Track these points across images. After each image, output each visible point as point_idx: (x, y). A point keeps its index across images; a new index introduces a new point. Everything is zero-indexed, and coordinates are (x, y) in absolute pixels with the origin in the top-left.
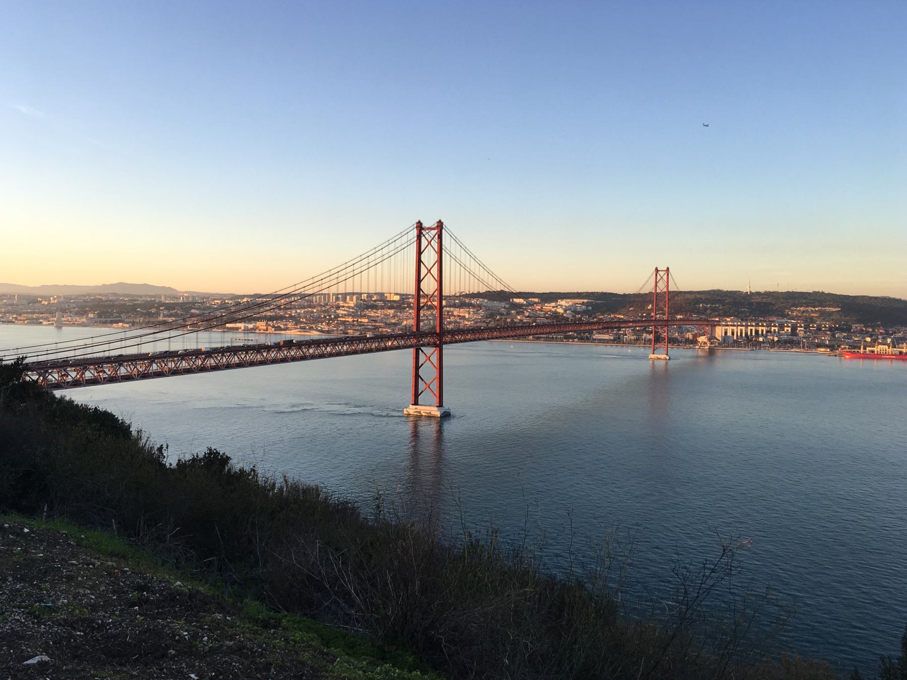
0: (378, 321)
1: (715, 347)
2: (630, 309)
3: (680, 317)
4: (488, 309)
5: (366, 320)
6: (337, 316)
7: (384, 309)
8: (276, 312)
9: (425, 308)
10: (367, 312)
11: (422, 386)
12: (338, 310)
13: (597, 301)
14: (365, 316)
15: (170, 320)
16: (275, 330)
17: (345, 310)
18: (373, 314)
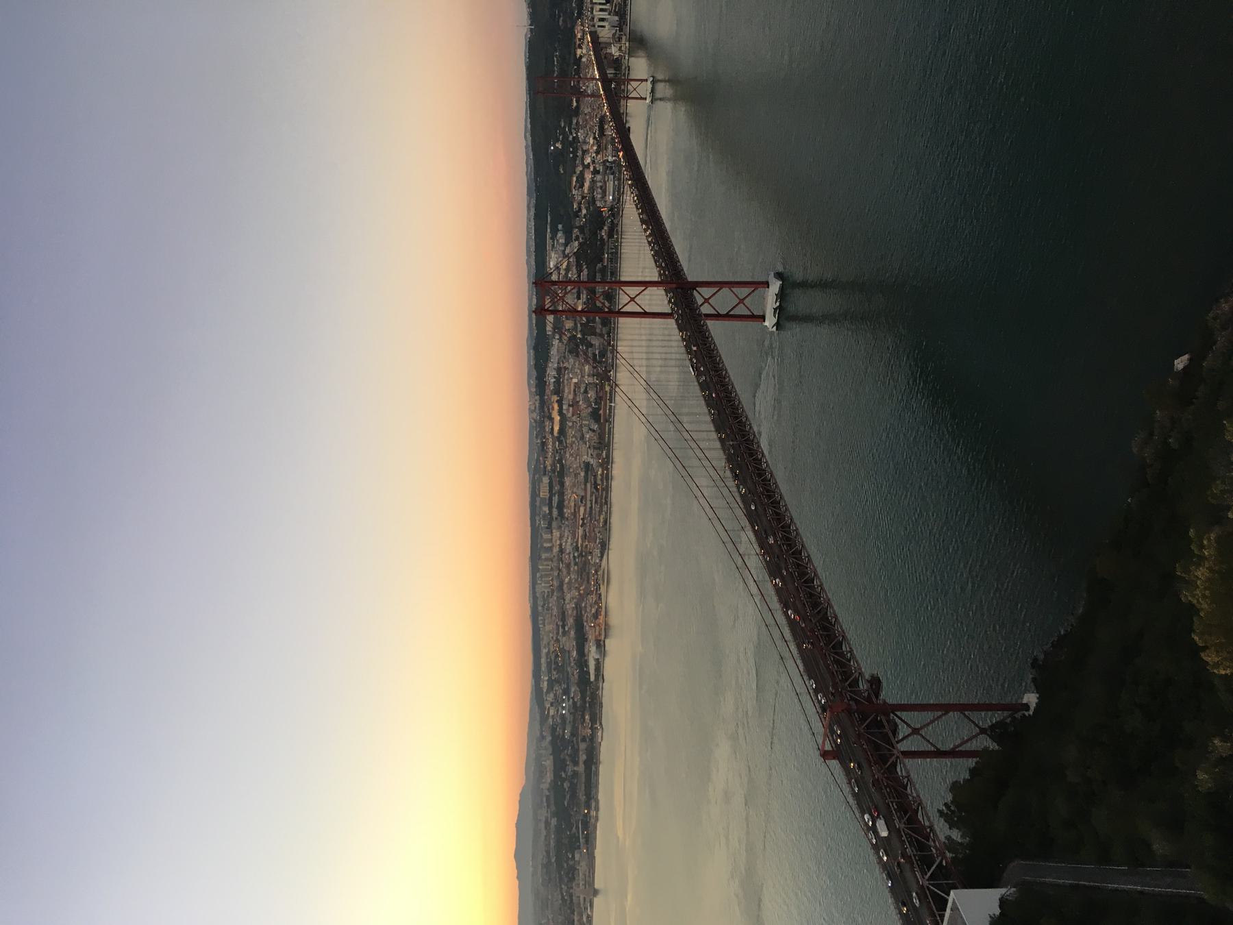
0: (583, 494)
1: (625, 35)
2: (562, 172)
3: (574, 101)
4: (563, 358)
5: (582, 509)
6: (577, 548)
7: (564, 493)
8: (569, 629)
9: (562, 438)
10: (567, 512)
11: (741, 310)
12: (566, 550)
13: (549, 217)
14: (575, 514)
15: (583, 757)
16: (601, 615)
17: (566, 542)
18: (573, 504)
